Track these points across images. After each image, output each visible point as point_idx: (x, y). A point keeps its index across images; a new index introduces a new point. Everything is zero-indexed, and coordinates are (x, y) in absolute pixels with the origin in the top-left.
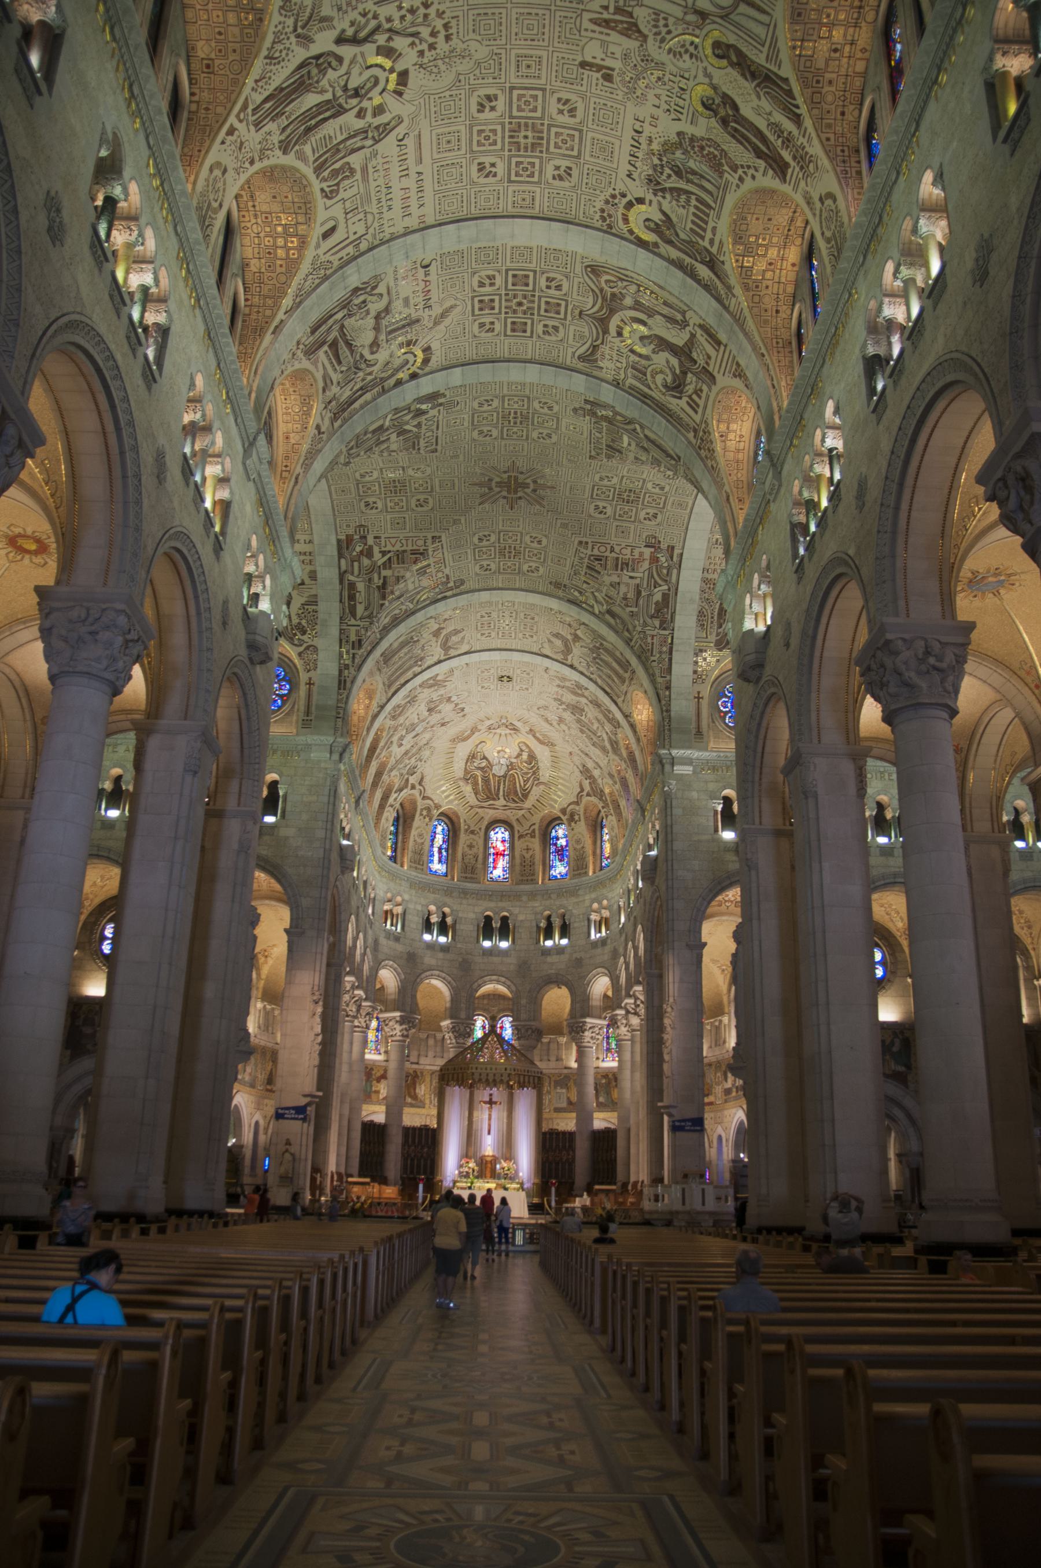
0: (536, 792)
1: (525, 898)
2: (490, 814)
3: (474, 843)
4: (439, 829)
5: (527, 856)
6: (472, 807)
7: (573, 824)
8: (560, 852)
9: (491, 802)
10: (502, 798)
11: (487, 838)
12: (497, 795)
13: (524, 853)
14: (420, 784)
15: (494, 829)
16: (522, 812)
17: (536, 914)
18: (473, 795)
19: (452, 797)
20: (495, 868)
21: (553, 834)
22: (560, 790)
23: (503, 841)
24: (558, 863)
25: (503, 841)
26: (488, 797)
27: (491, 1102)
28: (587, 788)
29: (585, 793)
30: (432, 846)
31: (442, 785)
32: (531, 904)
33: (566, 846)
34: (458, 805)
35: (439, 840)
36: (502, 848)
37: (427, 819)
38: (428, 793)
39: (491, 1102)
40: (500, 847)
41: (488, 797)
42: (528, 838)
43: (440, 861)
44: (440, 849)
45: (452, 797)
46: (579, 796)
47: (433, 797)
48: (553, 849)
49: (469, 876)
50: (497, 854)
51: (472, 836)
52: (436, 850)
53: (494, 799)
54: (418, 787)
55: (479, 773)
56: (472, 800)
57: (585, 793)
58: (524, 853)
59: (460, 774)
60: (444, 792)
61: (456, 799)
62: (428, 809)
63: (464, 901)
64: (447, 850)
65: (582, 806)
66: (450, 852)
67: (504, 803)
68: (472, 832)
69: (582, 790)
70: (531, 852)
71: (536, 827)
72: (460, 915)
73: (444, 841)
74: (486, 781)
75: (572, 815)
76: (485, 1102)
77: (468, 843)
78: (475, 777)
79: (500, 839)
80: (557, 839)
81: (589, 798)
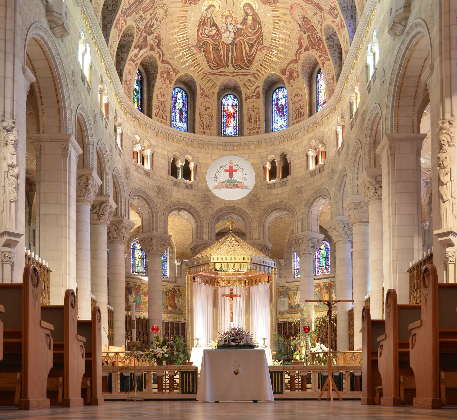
0: (259, 56)
1: (252, 147)
2: (221, 81)
3: (209, 105)
4: (179, 95)
5: (253, 114)
6: (206, 74)
7: (292, 81)
8: (281, 110)
9: (222, 69)
10: (230, 65)
11: (220, 105)
12: (227, 62)
13: (251, 111)
14: (158, 46)
15: (225, 97)
16: (249, 77)
17: (262, 158)
18: (206, 63)
19: (188, 64)
20: (227, 127)
21: (275, 96)
22: (281, 51)
23: (233, 106)
24: (279, 118)
25: (233, 106)
26: (219, 65)
27: (232, 296)
28: (306, 43)
29: (303, 49)
30: (174, 108)
31: (178, 52)
32: (257, 151)
33: (285, 104)
34: (194, 71)
35: (180, 104)
36: (232, 111)
37: (167, 82)
38: (167, 57)
39: (232, 296)
40: (231, 110)
41: (219, 65)
42: (254, 99)
43: (181, 120)
44: (181, 111)
45: (188, 64)
46: (298, 54)
47: (171, 62)
48: (274, 108)
49: (207, 131)
50: (228, 116)
51: (206, 99)
52: (177, 111)
53: (224, 67)
54: (157, 49)
55: (210, 40)
56: (206, 68)
57: (303, 49)
58: (251, 111)
59: (193, 41)
60: (180, 58)
61: (191, 65)
62: (168, 73)
63: (203, 151)
64: (187, 112)
65: (300, 62)
66: (189, 113)
67: (233, 70)
68: (207, 96)
69: (301, 46)
70: (256, 111)
71: (261, 89)
72: (200, 161)
73: (183, 105)
74: (217, 49)
75: (291, 74)
76: (227, 296)
77: (204, 105)
78: (206, 44)
79: (230, 104)
80: (278, 100)
81: (307, 53)
